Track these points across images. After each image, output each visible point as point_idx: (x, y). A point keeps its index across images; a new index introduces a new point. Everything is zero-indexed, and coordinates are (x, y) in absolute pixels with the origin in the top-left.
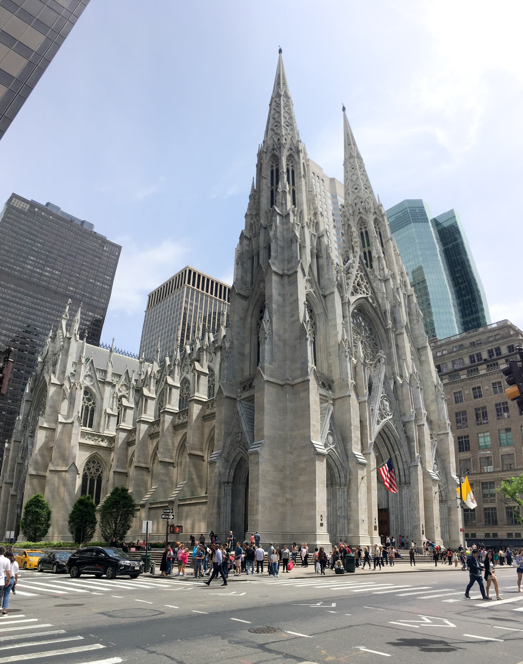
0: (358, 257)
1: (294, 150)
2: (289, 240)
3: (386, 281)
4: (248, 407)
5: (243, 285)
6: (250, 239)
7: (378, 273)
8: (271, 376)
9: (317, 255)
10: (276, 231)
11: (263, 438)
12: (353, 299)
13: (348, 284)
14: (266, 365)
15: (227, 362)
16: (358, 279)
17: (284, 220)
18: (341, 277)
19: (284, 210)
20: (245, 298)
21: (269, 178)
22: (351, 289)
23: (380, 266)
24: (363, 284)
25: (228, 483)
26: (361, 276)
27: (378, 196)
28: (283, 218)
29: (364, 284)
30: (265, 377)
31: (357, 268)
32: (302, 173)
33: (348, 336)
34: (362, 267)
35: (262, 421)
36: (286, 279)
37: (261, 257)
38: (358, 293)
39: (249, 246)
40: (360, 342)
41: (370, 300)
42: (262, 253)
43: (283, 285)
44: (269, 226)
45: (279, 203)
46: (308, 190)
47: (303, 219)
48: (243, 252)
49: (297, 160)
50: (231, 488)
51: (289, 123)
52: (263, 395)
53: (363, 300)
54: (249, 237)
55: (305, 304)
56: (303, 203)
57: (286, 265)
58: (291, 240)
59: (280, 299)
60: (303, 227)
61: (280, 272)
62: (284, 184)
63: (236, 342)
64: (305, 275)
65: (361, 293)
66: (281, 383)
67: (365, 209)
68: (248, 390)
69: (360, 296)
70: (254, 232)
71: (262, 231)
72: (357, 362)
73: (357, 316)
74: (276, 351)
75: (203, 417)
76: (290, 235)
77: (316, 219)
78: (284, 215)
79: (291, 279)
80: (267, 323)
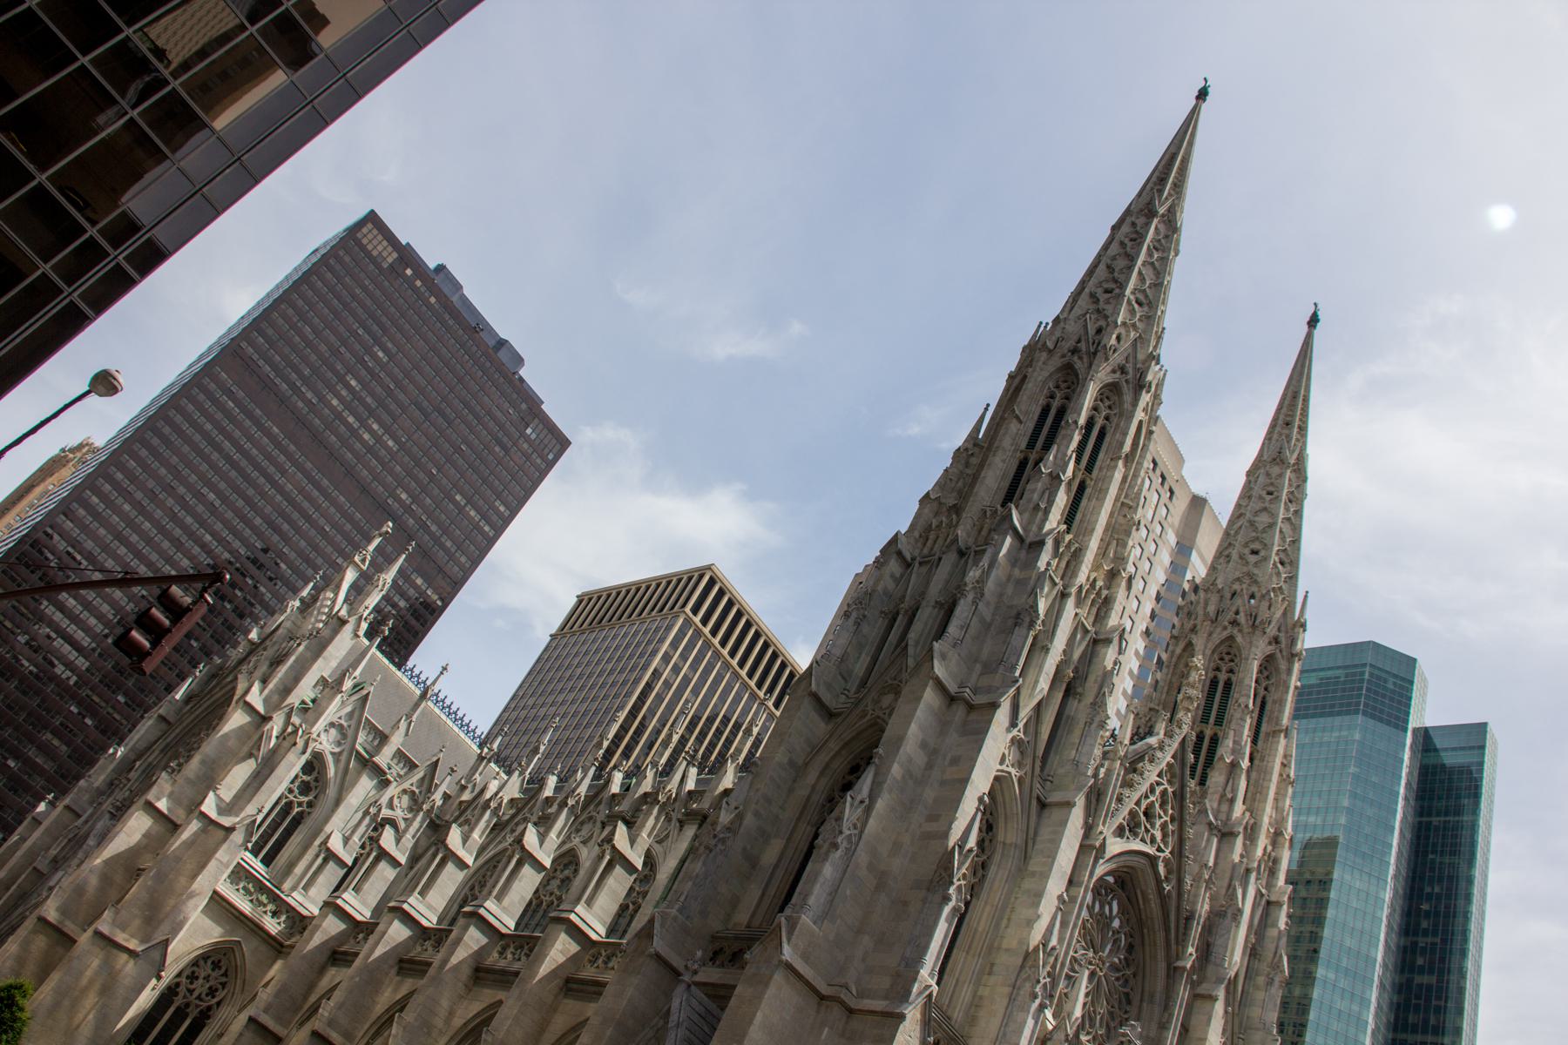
0: (1178, 739)
1: (1130, 376)
2: (1014, 612)
3: (1226, 835)
4: (702, 1010)
5: (840, 678)
6: (908, 565)
7: (1215, 805)
8: (805, 957)
9: (1069, 684)
10: (986, 573)
12: (1115, 846)
13: (1119, 800)
14: (806, 919)
15: (704, 864)
16: (1152, 798)
17: (1023, 554)
18: (1109, 772)
19: (1034, 528)
20: (829, 714)
21: (1030, 425)
22: (1121, 817)
23: (1229, 788)
24: (1160, 817)
26: (1164, 792)
27: (1306, 597)
28: (1020, 549)
29: (1165, 818)
30: (788, 953)
31: (1163, 765)
32: (1127, 448)
33: (1061, 940)
34: (1177, 770)
36: (959, 712)
37: (917, 626)
38: (1136, 835)
39: (897, 581)
40: (1087, 973)
41: (1161, 869)
42: (926, 617)
43: (943, 725)
44: (975, 552)
45: (1030, 500)
46: (1122, 500)
47: (1074, 574)
48: (873, 591)
49: (1127, 406)
53: (1143, 860)
54: (908, 557)
55: (981, 800)
57: (974, 676)
58: (1018, 616)
59: (920, 759)
60: (1064, 595)
61: (952, 688)
62: (1065, 460)
63: (749, 820)
64: (1013, 724)
65: (1143, 840)
66: (824, 989)
67: (1253, 617)
68: (722, 965)
69: (1136, 845)
70: (926, 551)
71: (950, 559)
72: (1055, 1028)
73: (1107, 895)
74: (848, 892)
75: (568, 980)
76: (1021, 601)
77: (1108, 589)
78: (1028, 541)
79: (974, 716)
80: (857, 808)
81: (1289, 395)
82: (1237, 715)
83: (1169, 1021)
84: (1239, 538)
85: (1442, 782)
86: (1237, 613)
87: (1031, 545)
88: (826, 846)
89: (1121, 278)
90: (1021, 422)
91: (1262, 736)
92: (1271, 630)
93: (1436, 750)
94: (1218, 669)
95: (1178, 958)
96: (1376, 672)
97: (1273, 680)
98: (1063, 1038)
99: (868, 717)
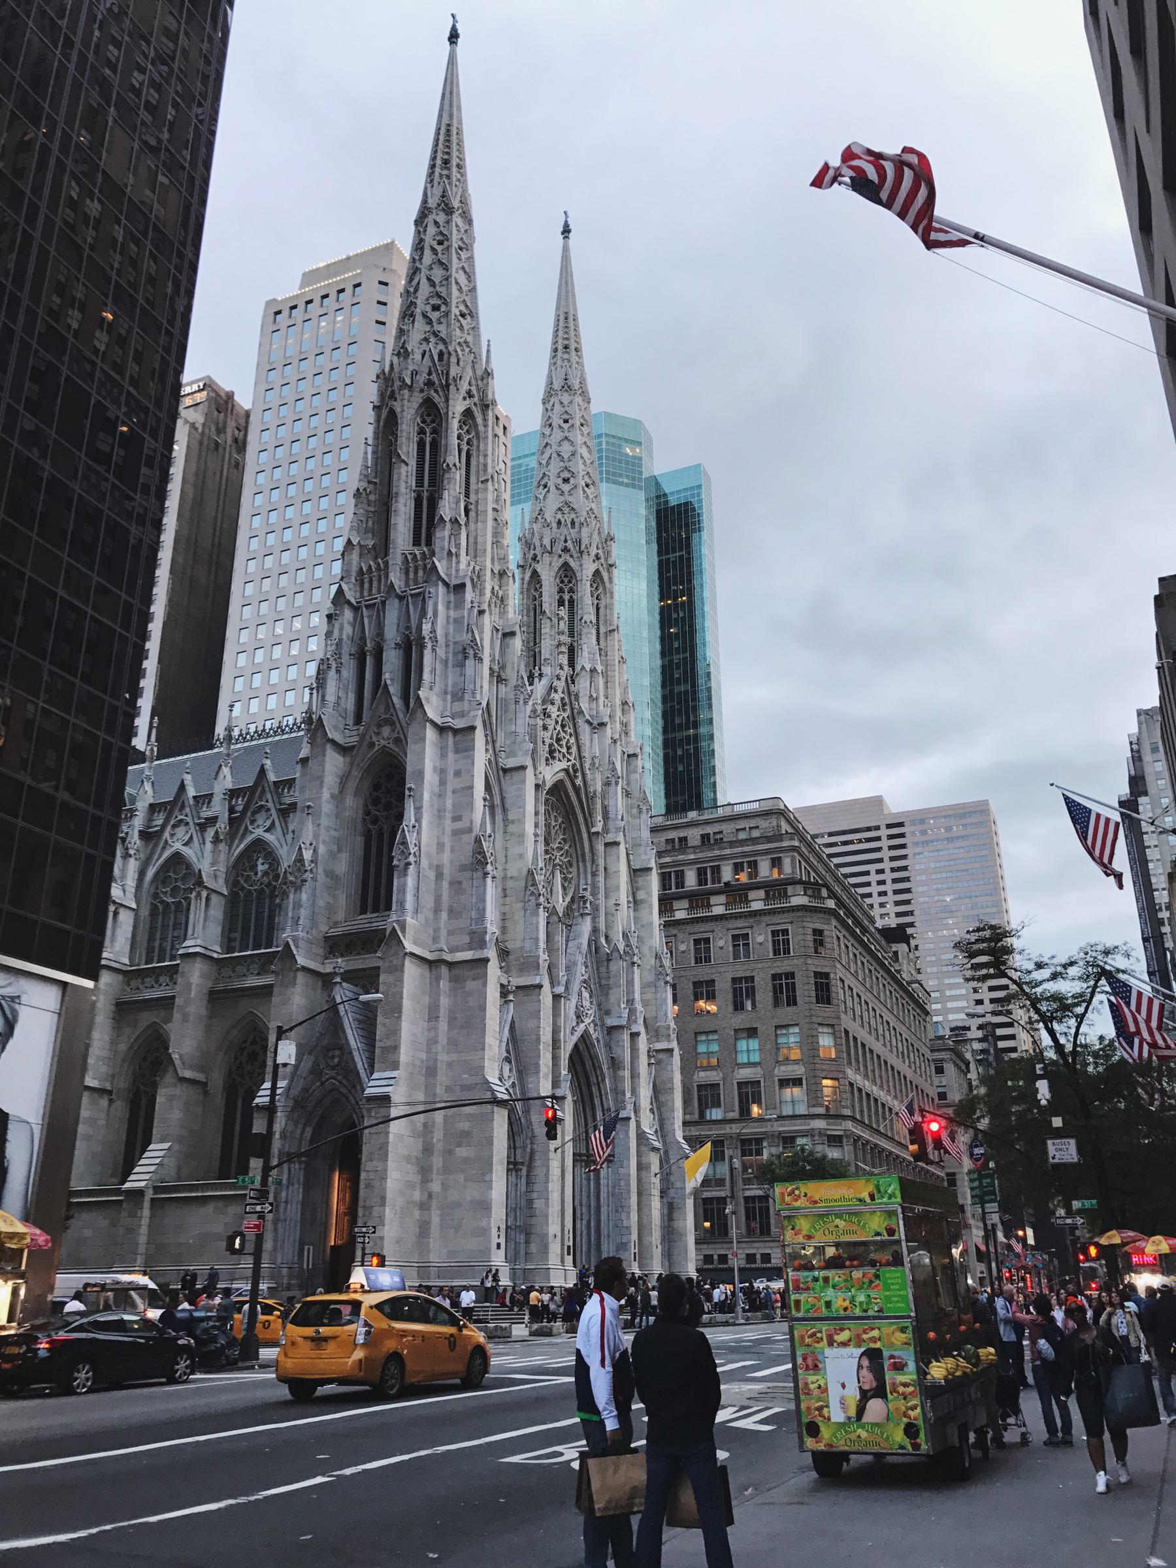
1: (476, 399)
2: (460, 649)
6: (356, 609)
11: (395, 1066)
21: (413, 463)
30: (409, 946)
34: (567, 700)
35: (395, 1032)
42: (392, 660)
45: (443, 549)
47: (482, 594)
49: (481, 428)
51: (467, 306)
52: (401, 981)
63: (322, 849)
76: (465, 637)
79: (459, 737)
81: (562, 318)
82: (585, 630)
86: (566, 541)
88: (402, 865)
89: (442, 290)
90: (407, 464)
91: (602, 636)
92: (594, 551)
93: (665, 495)
94: (561, 591)
96: (612, 440)
97: (601, 589)
99: (377, 748)
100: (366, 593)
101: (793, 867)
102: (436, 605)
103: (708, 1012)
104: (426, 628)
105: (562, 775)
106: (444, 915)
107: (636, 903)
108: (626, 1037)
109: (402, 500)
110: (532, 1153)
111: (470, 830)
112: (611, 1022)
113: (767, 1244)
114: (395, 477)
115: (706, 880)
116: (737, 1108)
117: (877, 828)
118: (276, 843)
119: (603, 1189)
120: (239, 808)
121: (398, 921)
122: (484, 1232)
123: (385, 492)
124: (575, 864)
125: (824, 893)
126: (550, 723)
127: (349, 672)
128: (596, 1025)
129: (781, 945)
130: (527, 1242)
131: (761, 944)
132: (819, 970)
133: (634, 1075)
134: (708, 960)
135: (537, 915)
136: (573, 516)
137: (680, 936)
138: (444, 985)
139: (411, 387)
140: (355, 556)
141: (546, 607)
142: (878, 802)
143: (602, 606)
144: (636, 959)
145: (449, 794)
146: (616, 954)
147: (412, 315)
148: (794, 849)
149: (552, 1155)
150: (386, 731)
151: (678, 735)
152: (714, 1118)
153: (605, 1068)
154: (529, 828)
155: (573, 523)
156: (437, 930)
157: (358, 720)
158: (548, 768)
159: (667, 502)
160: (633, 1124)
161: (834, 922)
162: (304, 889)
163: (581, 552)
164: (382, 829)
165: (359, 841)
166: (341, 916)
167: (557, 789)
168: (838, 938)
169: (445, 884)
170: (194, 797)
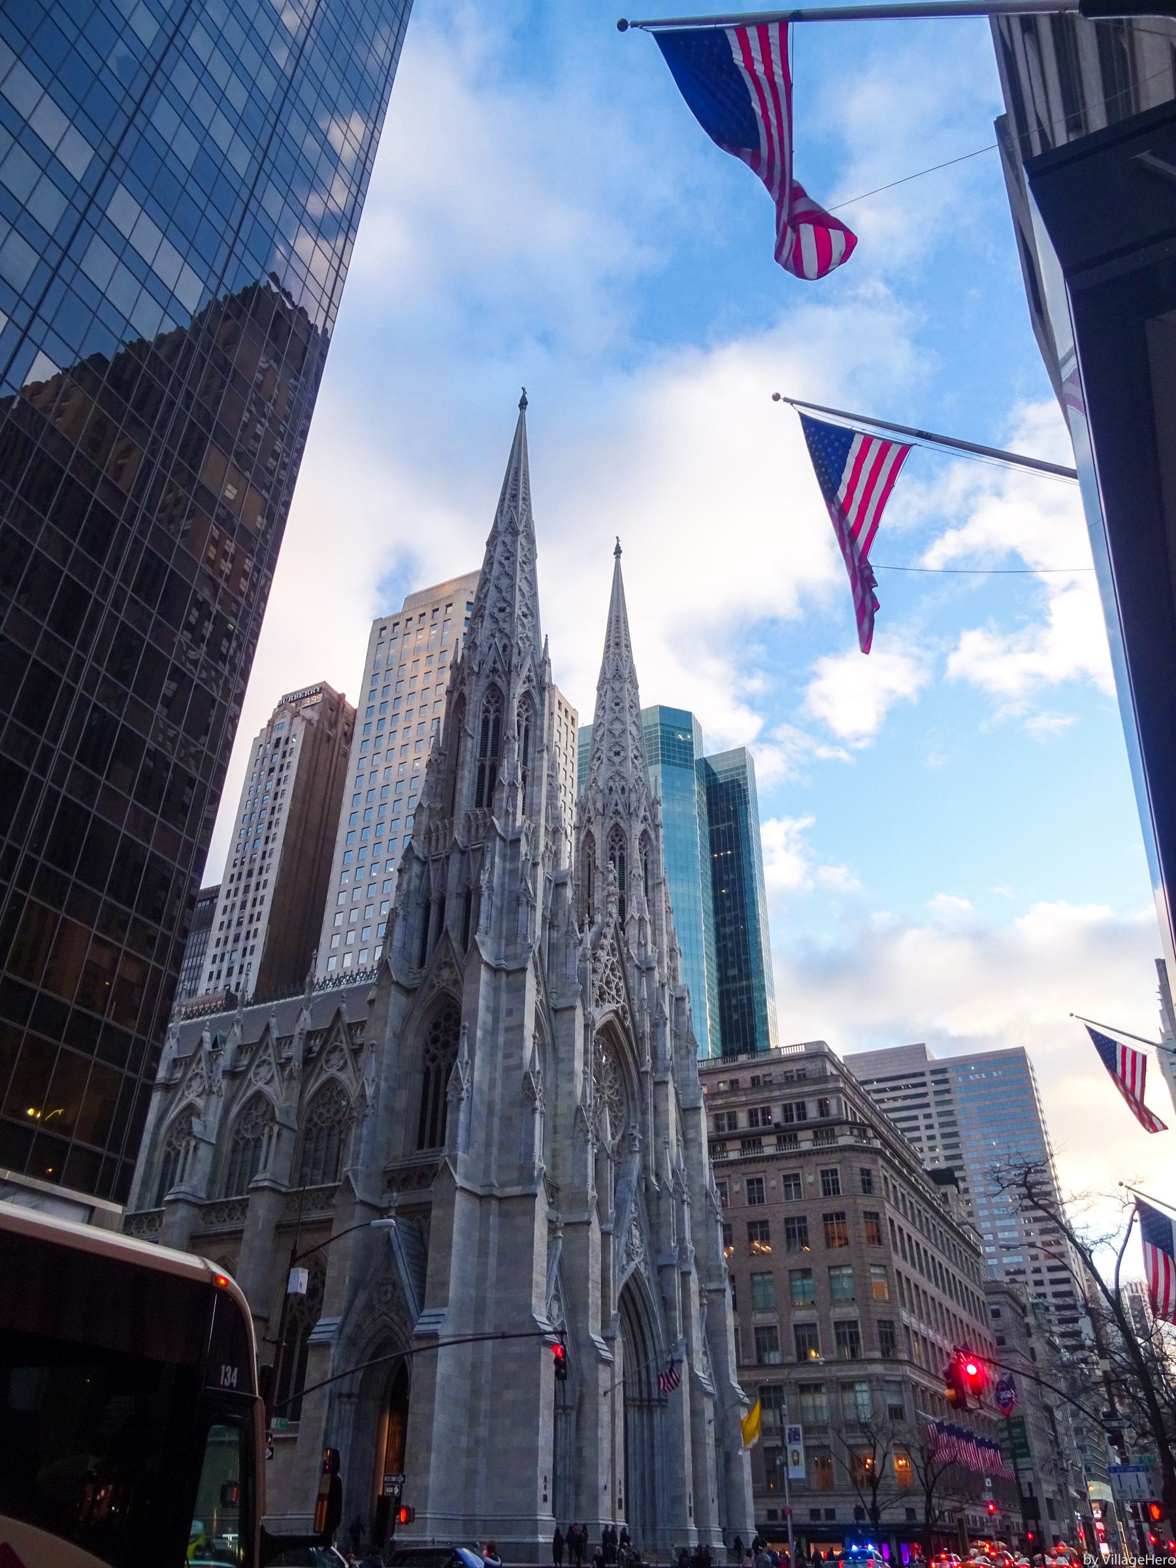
1: (534, 683)
4: (405, 1229)
6: (424, 863)
10: (491, 873)
11: (445, 1304)
21: (478, 737)
25: (349, 1396)
30: (459, 1180)
35: (446, 1268)
42: (453, 909)
45: (501, 808)
47: (536, 847)
49: (538, 707)
50: (354, 1407)
56: (539, 811)
58: (518, 899)
63: (383, 1085)
66: (479, 1191)
67: (627, 806)
71: (455, 859)
75: (278, 1227)
79: (511, 978)
82: (634, 883)
83: (647, 1109)
84: (604, 743)
85: (722, 797)
86: (617, 805)
87: (511, 841)
88: (455, 1101)
89: (508, 596)
91: (650, 889)
92: (642, 814)
93: (714, 774)
94: (612, 848)
95: (642, 1065)
96: (666, 728)
98: (605, 1156)
100: (433, 849)
101: (840, 1108)
102: (493, 857)
103: (763, 1252)
104: (484, 877)
105: (611, 1016)
106: (495, 1150)
107: (687, 1142)
108: (677, 1277)
109: (467, 768)
110: (581, 1397)
111: (520, 1066)
112: (662, 1261)
113: (832, 1499)
114: (462, 749)
115: (757, 1121)
116: (794, 1352)
117: (922, 1074)
118: (348, 1083)
119: (658, 1437)
120: (316, 1049)
121: (449, 1156)
122: (531, 1482)
123: (454, 762)
124: (625, 1100)
125: (870, 1133)
126: (600, 966)
127: (416, 921)
128: (646, 1264)
129: (831, 1186)
130: (577, 1494)
131: (811, 1184)
132: (868, 1209)
133: (686, 1316)
134: (761, 1200)
135: (586, 1151)
136: (623, 783)
137: (733, 1176)
138: (493, 1220)
139: (478, 674)
140: (424, 818)
141: (598, 863)
142: (920, 1050)
143: (649, 861)
144: (685, 1197)
145: (502, 1032)
146: (665, 1191)
147: (482, 617)
148: (839, 1090)
149: (601, 1400)
150: (446, 973)
151: (732, 986)
152: (772, 1362)
153: (656, 1309)
154: (579, 1065)
155: (623, 789)
156: (487, 1166)
157: (422, 964)
158: (598, 1010)
159: (716, 780)
160: (685, 1367)
161: (881, 1162)
162: (365, 1124)
163: (630, 814)
164: (439, 1066)
165: (418, 1078)
166: (398, 1151)
167: (608, 1030)
168: (886, 1178)
169: (496, 1121)
170: (278, 1039)
